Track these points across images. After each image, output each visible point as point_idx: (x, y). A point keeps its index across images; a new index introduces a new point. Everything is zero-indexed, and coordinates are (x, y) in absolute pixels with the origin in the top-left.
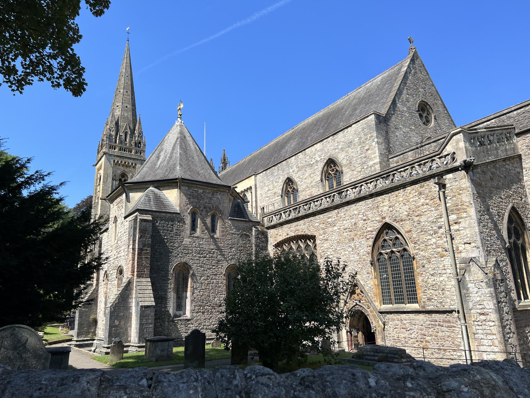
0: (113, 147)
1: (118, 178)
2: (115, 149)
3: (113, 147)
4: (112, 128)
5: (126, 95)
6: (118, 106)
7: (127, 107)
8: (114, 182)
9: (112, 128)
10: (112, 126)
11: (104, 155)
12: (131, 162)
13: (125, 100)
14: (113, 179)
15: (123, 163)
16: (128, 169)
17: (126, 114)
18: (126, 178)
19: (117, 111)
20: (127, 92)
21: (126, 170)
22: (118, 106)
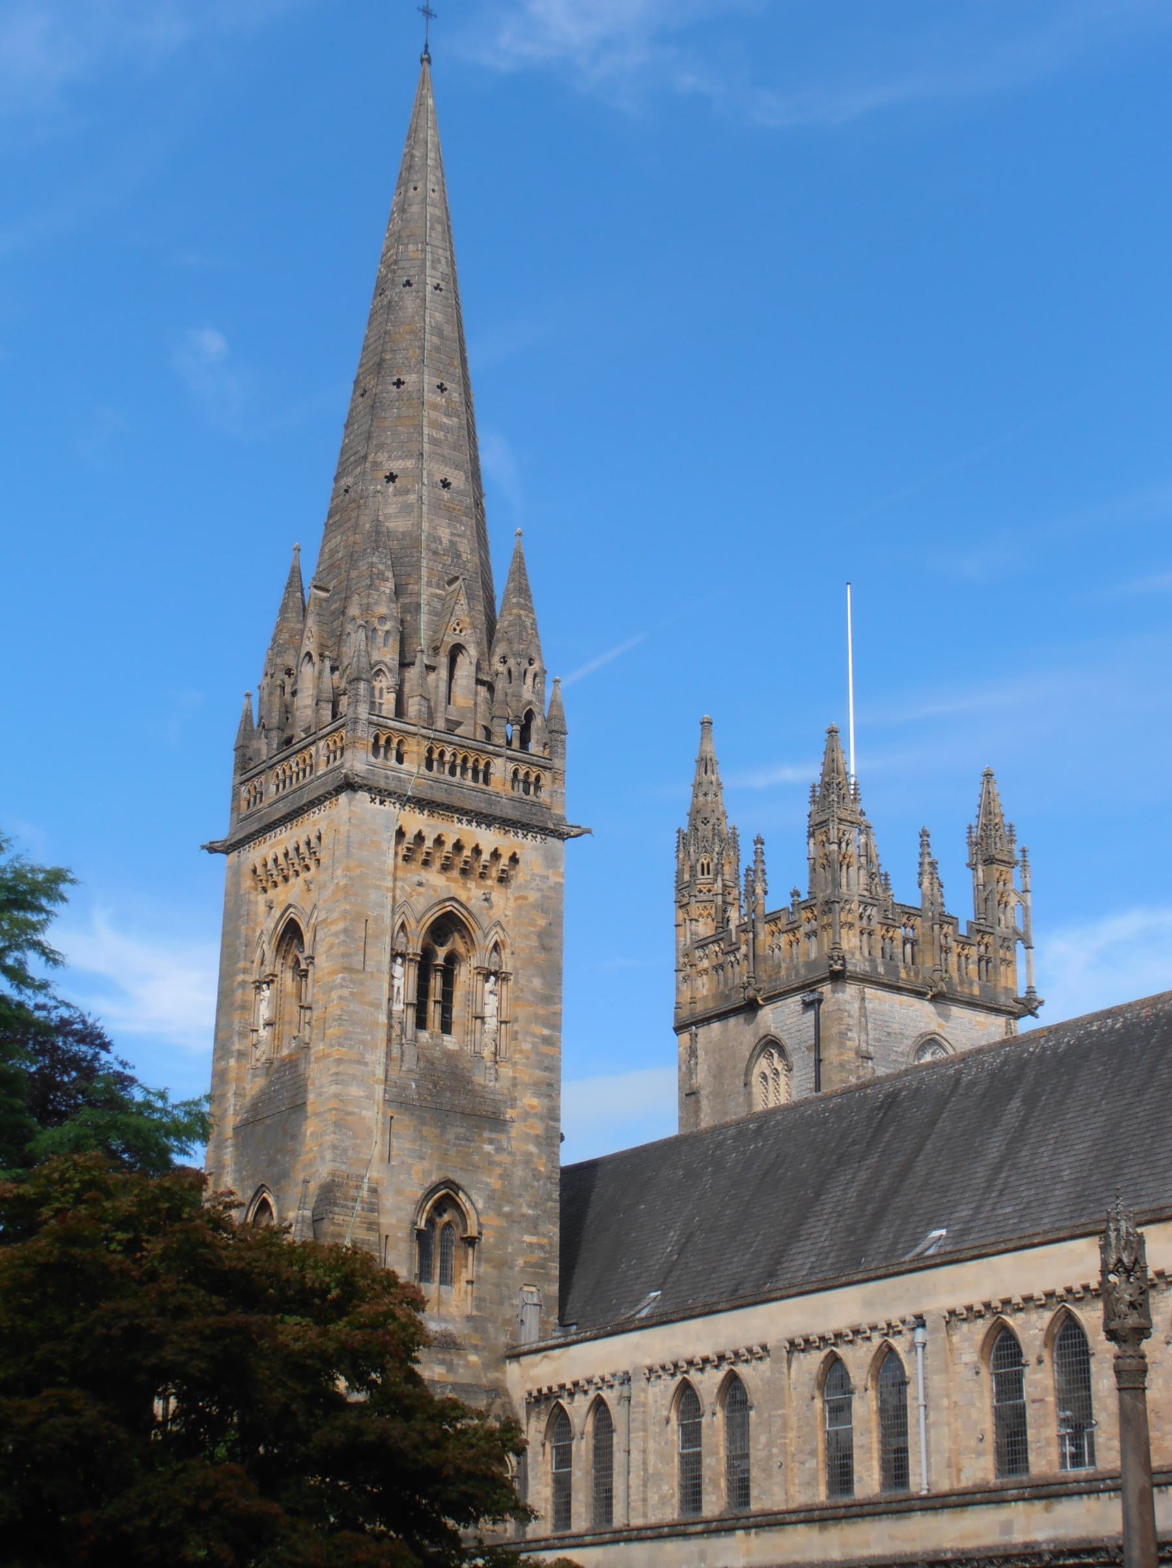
0: (388, 741)
1: (415, 947)
2: (400, 759)
3: (388, 741)
4: (383, 619)
5: (435, 407)
6: (391, 478)
7: (446, 484)
8: (398, 970)
9: (383, 619)
10: (382, 610)
11: (338, 790)
12: (488, 838)
13: (434, 442)
14: (395, 955)
15: (448, 847)
16: (472, 885)
17: (445, 533)
18: (461, 948)
19: (392, 510)
20: (441, 387)
21: (462, 895)
22: (391, 478)
